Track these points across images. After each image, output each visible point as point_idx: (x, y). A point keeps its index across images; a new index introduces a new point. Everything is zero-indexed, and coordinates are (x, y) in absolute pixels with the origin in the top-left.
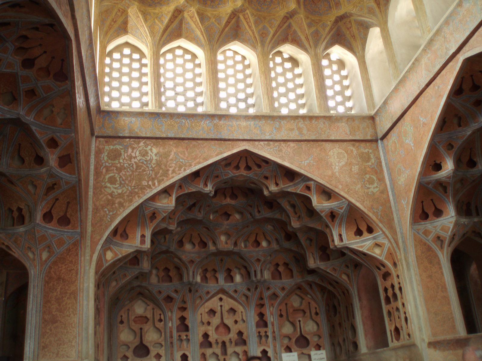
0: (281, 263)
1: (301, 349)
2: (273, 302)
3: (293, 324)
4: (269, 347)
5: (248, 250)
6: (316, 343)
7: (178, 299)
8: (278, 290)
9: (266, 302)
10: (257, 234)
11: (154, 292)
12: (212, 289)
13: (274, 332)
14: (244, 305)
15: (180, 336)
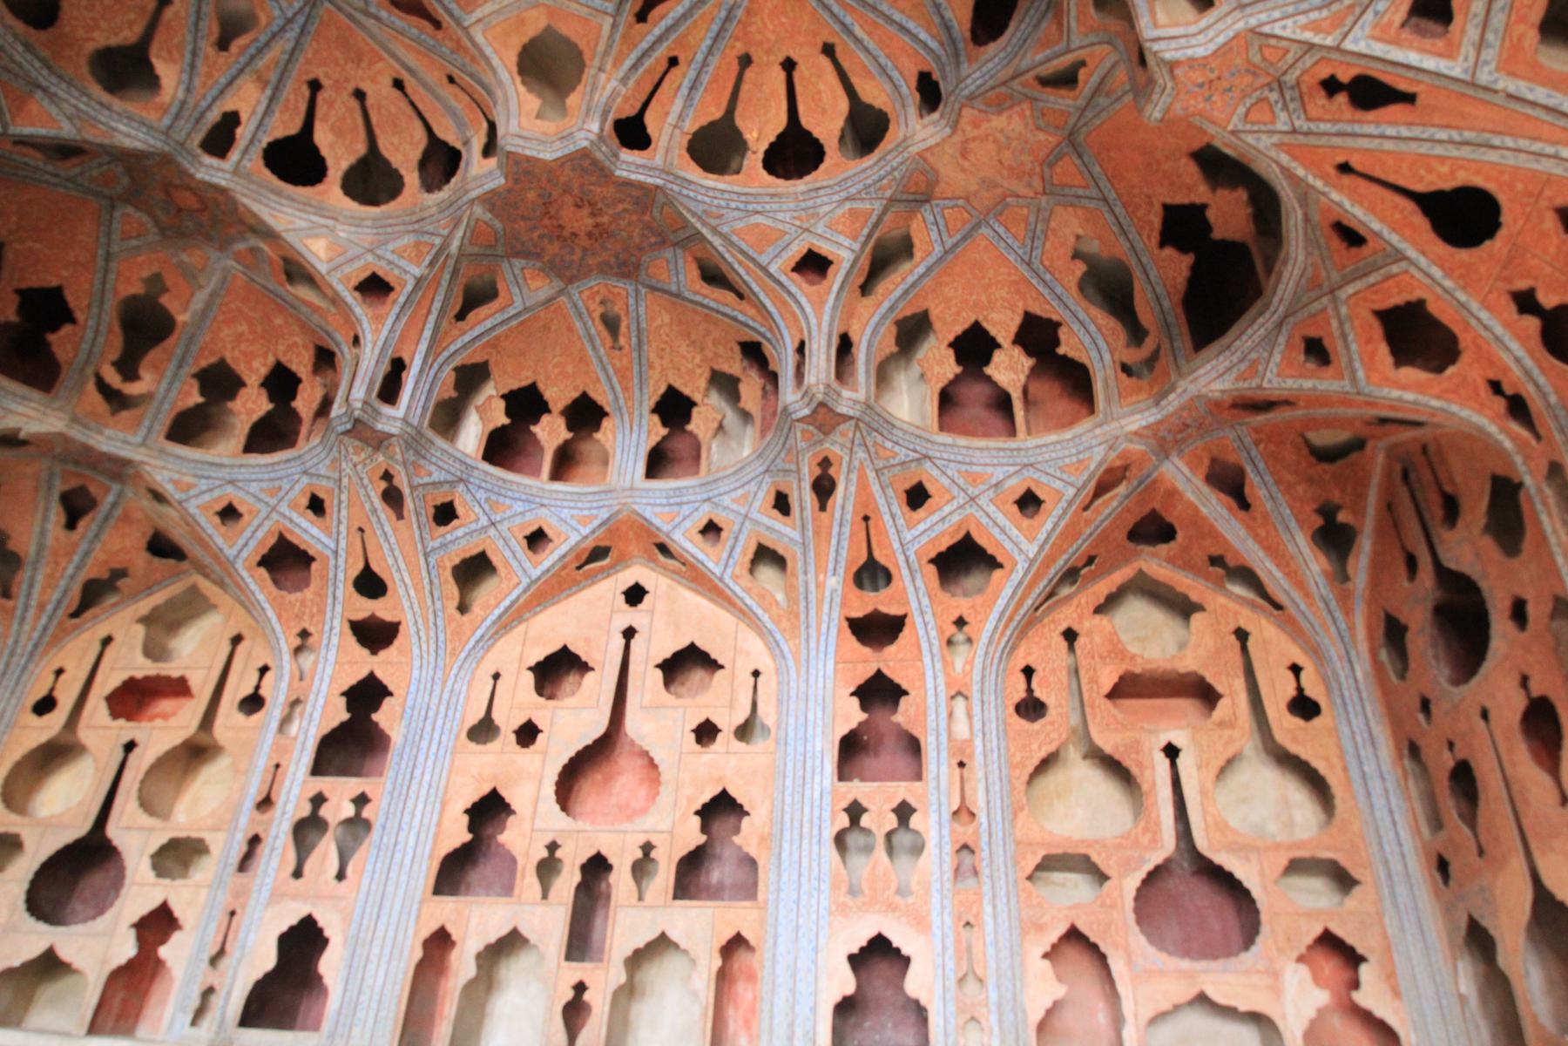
0: (1003, 326)
1: (1185, 964)
2: (960, 604)
3: (1115, 768)
4: (921, 922)
5: (737, 189)
6: (1317, 930)
7: (336, 553)
8: (991, 509)
9: (915, 593)
10: (789, 65)
11: (193, 510)
12: (565, 513)
13: (964, 813)
14: (770, 625)
15: (318, 800)
